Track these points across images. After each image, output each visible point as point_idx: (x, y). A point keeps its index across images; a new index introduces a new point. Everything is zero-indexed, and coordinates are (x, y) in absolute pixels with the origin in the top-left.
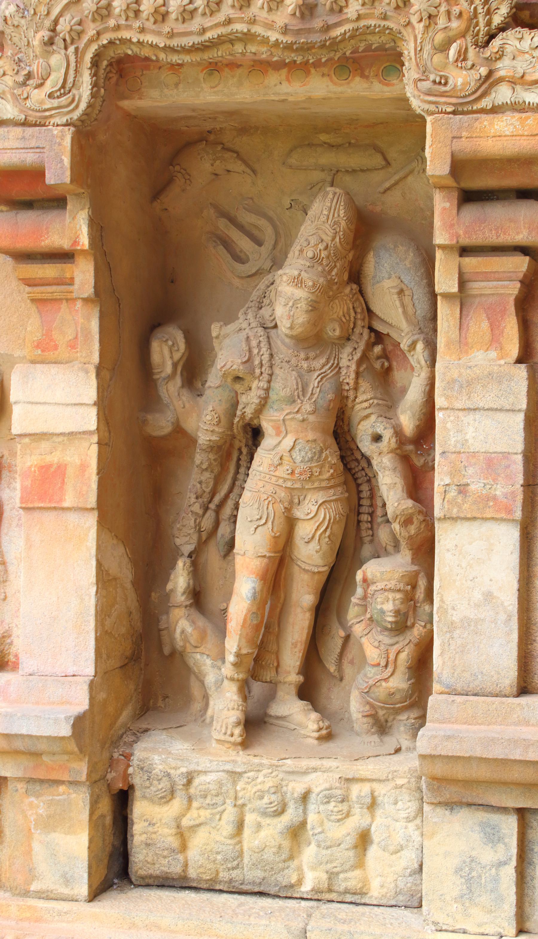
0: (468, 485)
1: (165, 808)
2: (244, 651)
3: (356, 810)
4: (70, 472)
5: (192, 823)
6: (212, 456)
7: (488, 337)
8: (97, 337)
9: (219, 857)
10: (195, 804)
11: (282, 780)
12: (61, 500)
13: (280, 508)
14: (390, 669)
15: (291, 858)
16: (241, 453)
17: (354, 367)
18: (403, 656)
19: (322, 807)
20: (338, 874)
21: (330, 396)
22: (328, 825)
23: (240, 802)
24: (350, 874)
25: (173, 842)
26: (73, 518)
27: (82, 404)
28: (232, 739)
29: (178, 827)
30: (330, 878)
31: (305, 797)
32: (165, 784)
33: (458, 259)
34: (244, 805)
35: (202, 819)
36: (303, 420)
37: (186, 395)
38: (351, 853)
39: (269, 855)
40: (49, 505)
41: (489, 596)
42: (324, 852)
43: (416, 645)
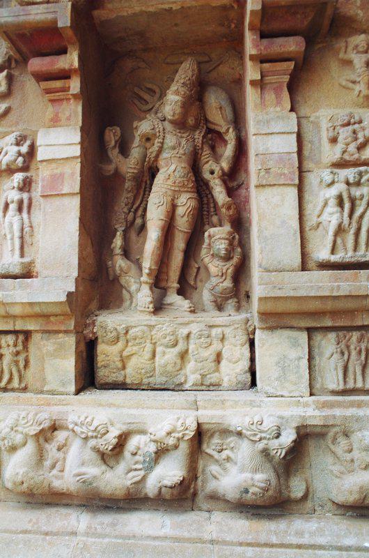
0: (270, 169)
1: (115, 346)
2: (153, 267)
3: (215, 342)
4: (66, 176)
5: (129, 354)
6: (133, 184)
7: (275, 102)
8: (81, 114)
9: (143, 371)
10: (130, 344)
11: (176, 328)
12: (62, 190)
13: (170, 198)
14: (224, 277)
15: (181, 369)
16: (146, 182)
17: (201, 138)
18: (230, 271)
19: (197, 341)
20: (206, 375)
21: (191, 149)
22: (200, 350)
23: (153, 341)
24: (212, 375)
25: (120, 365)
26: (66, 200)
27: (72, 144)
28: (147, 310)
29: (121, 356)
30: (202, 378)
31: (188, 336)
32: (114, 334)
33: (260, 65)
34: (156, 343)
35: (134, 352)
36: (180, 157)
37: (121, 157)
38: (213, 364)
39: (169, 368)
40: (55, 193)
41: (284, 222)
42: (199, 364)
43: (235, 266)
